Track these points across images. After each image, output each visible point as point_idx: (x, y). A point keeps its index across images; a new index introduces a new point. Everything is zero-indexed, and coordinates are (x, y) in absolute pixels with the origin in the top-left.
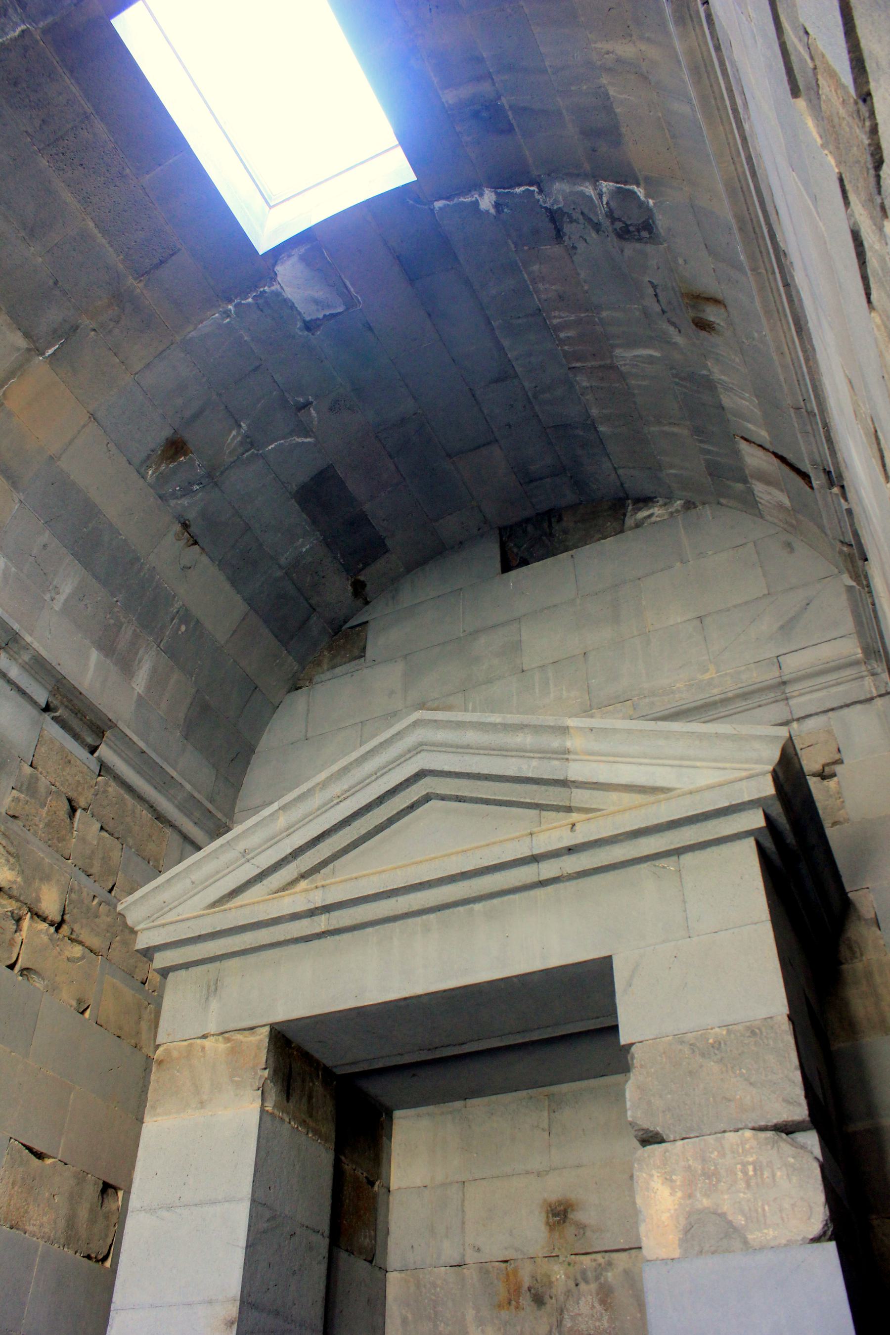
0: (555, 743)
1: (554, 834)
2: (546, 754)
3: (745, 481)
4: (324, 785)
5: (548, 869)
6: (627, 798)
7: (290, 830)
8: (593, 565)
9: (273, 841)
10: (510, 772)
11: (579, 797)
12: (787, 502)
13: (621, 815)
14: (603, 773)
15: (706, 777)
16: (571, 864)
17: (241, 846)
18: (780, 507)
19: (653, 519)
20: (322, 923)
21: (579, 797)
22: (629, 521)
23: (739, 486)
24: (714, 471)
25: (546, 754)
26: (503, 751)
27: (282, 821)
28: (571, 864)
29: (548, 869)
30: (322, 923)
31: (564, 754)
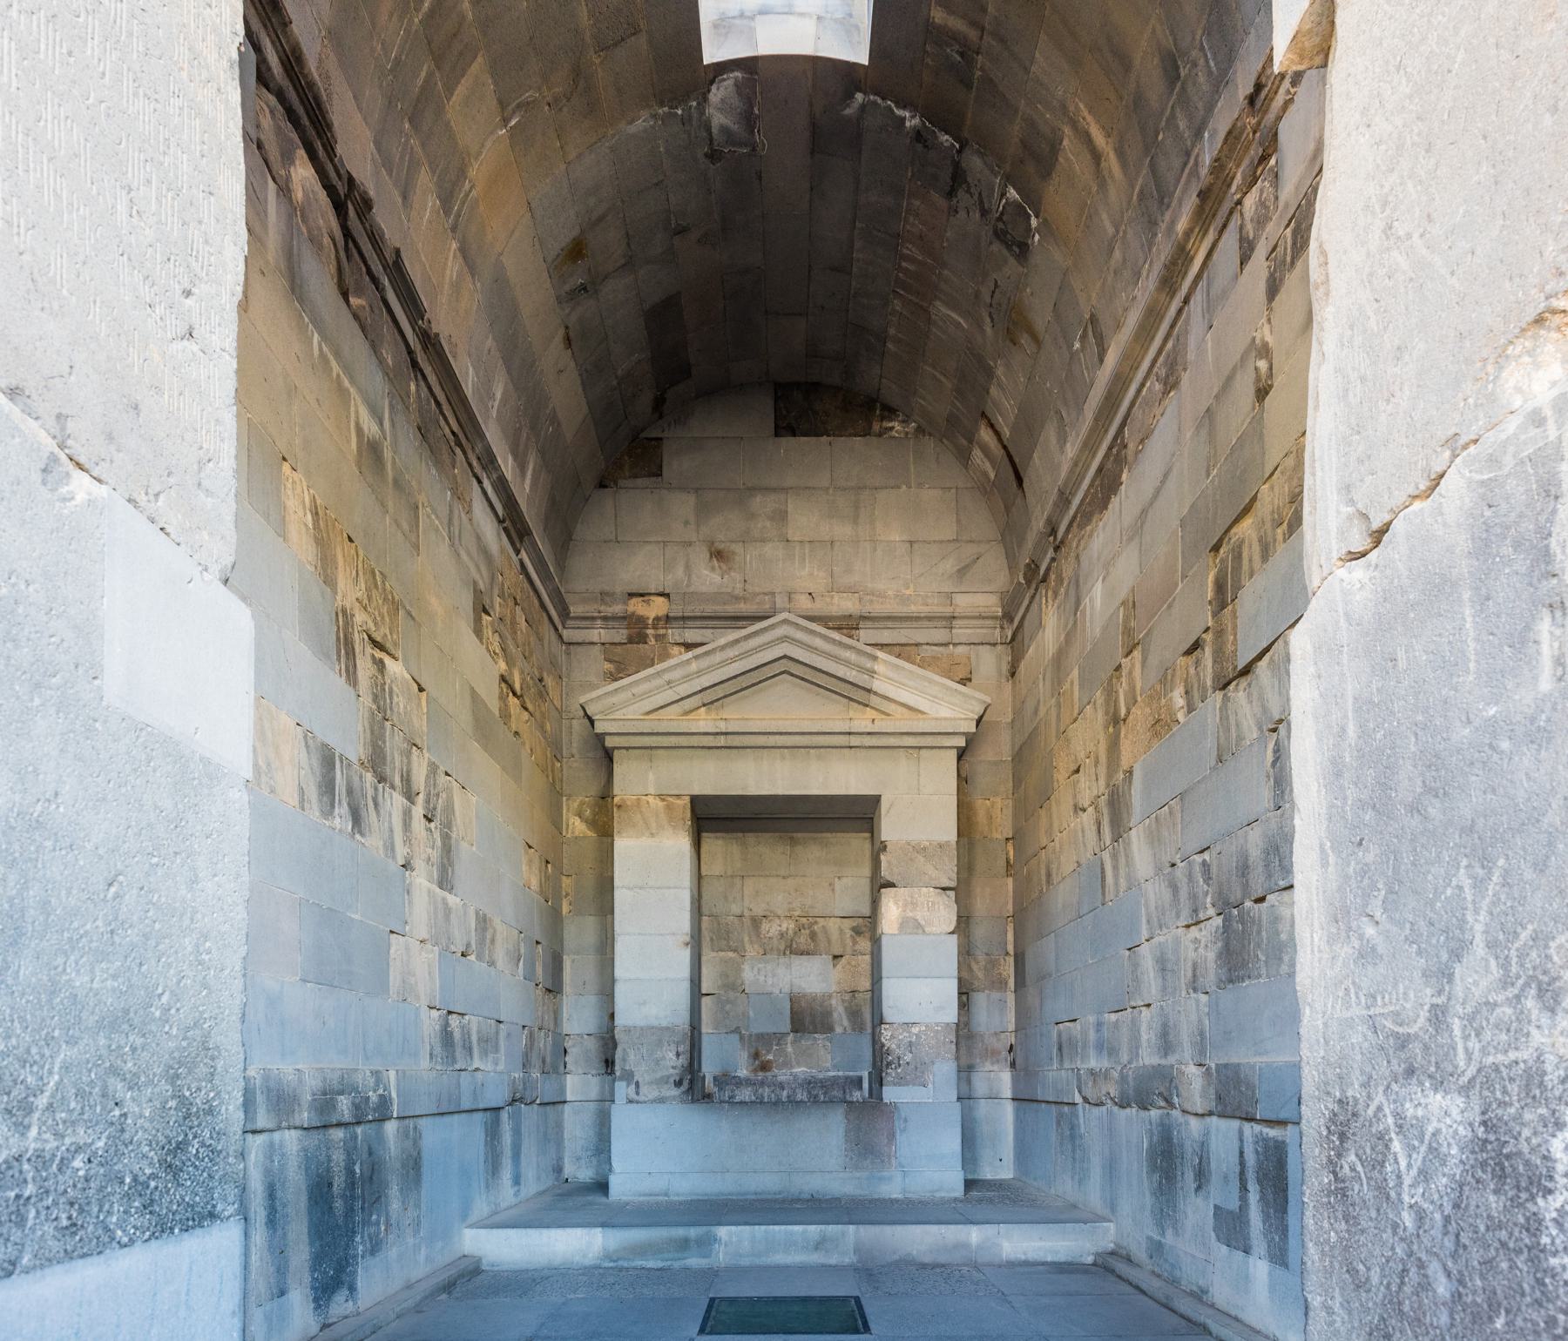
0: (869, 665)
1: (862, 720)
2: (862, 669)
3: (971, 441)
4: (723, 648)
5: (855, 741)
6: (900, 709)
7: (700, 673)
8: (847, 456)
9: (687, 678)
10: (840, 674)
11: (874, 700)
12: (992, 476)
13: (900, 722)
14: (891, 691)
15: (945, 712)
16: (868, 741)
17: (667, 677)
18: (985, 474)
19: (894, 433)
20: (722, 741)
21: (874, 700)
22: (876, 427)
23: (965, 442)
24: (953, 421)
25: (862, 669)
26: (836, 659)
27: (694, 666)
28: (868, 741)
29: (855, 741)
30: (722, 741)
31: (872, 673)
